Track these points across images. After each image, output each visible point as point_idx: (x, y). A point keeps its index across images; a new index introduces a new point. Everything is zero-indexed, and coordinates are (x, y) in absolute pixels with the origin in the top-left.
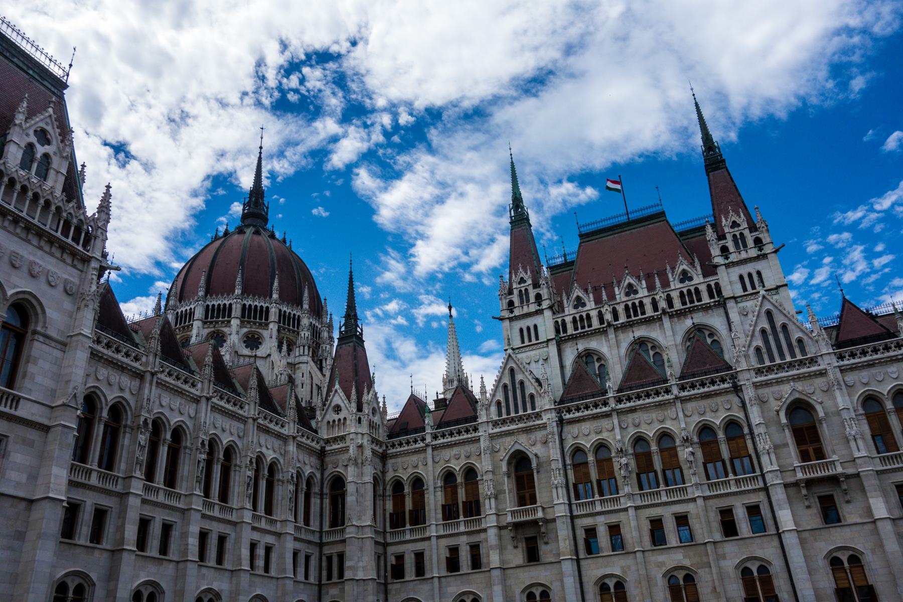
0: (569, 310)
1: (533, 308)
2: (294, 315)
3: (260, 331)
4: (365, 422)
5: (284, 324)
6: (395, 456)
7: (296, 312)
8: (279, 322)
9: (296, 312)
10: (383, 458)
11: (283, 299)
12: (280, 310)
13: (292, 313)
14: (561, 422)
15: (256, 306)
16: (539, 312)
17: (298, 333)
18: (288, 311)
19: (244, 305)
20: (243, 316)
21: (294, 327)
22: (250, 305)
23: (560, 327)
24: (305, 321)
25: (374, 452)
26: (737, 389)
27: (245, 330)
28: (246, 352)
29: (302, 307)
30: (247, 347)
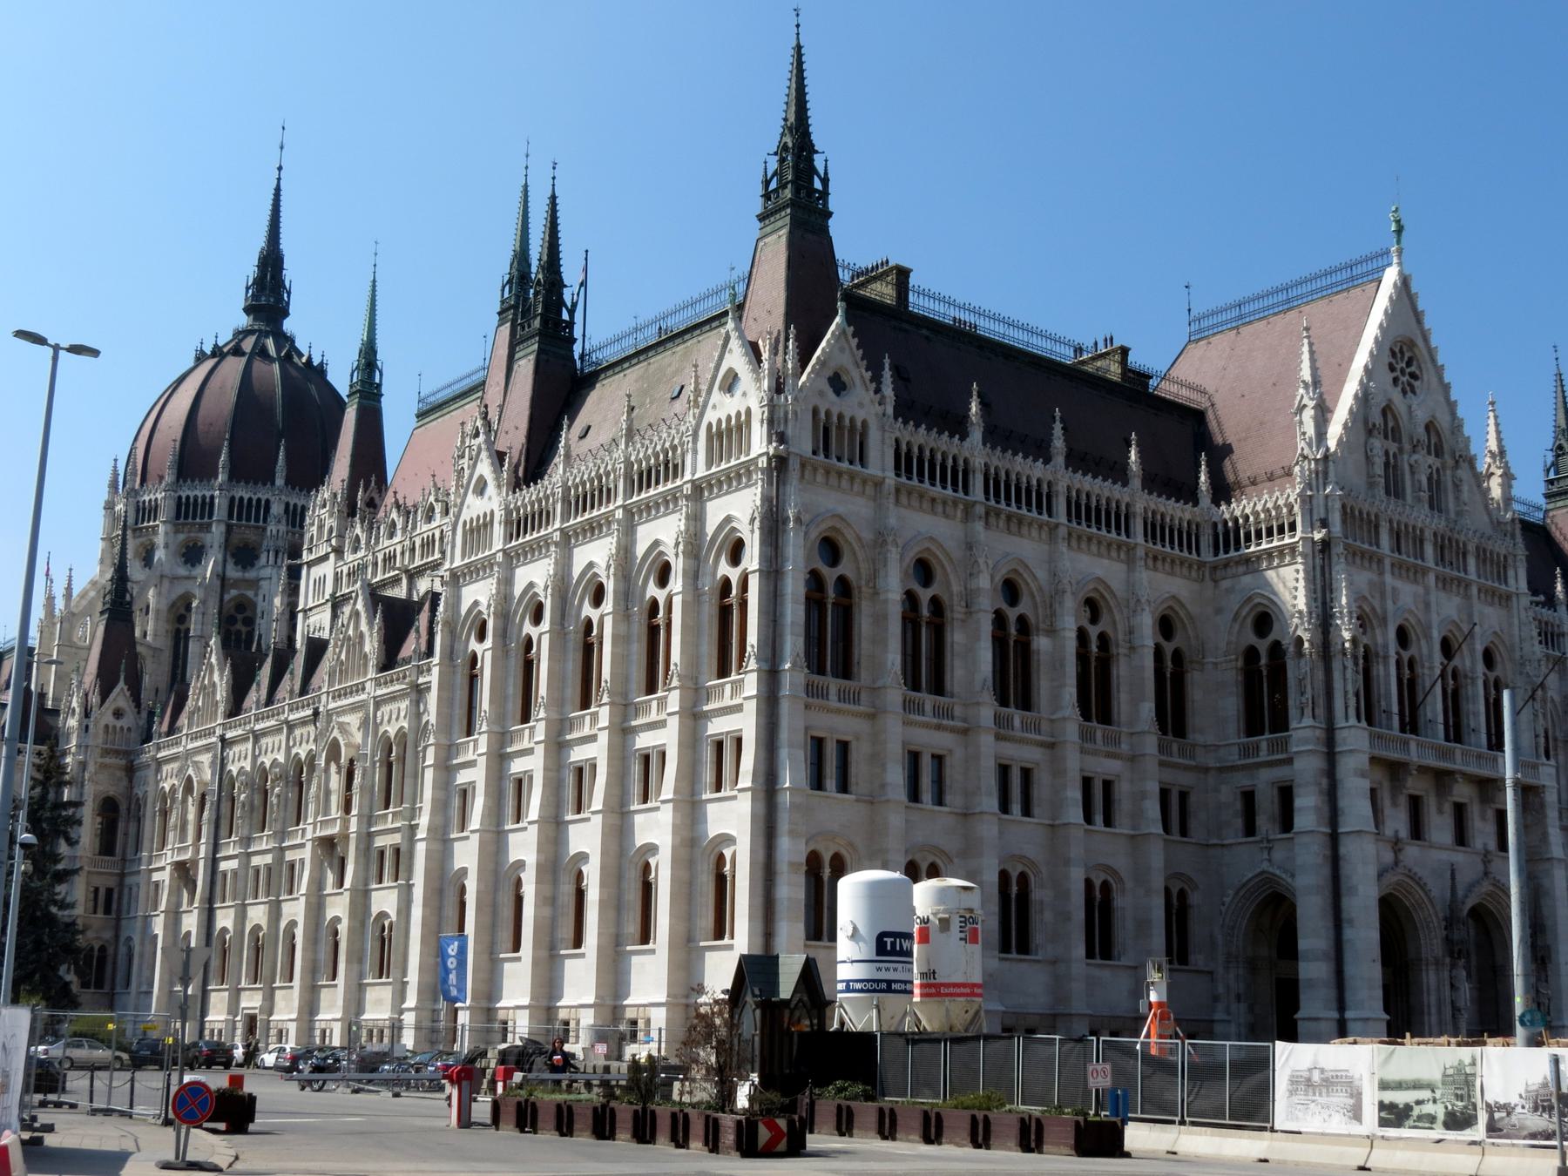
0: (349, 557)
1: (323, 549)
2: (259, 500)
3: (201, 535)
4: (97, 729)
5: (239, 518)
6: (139, 769)
7: (263, 495)
8: (230, 516)
9: (263, 495)
10: (131, 770)
11: (235, 475)
12: (233, 498)
13: (255, 498)
14: (223, 739)
15: (196, 498)
16: (325, 558)
17: (264, 529)
18: (246, 497)
19: (180, 498)
20: (178, 516)
21: (257, 520)
22: (188, 498)
23: (337, 578)
24: (277, 509)
25: (103, 766)
26: (316, 713)
27: (181, 537)
28: (182, 571)
29: (273, 483)
30: (186, 563)
